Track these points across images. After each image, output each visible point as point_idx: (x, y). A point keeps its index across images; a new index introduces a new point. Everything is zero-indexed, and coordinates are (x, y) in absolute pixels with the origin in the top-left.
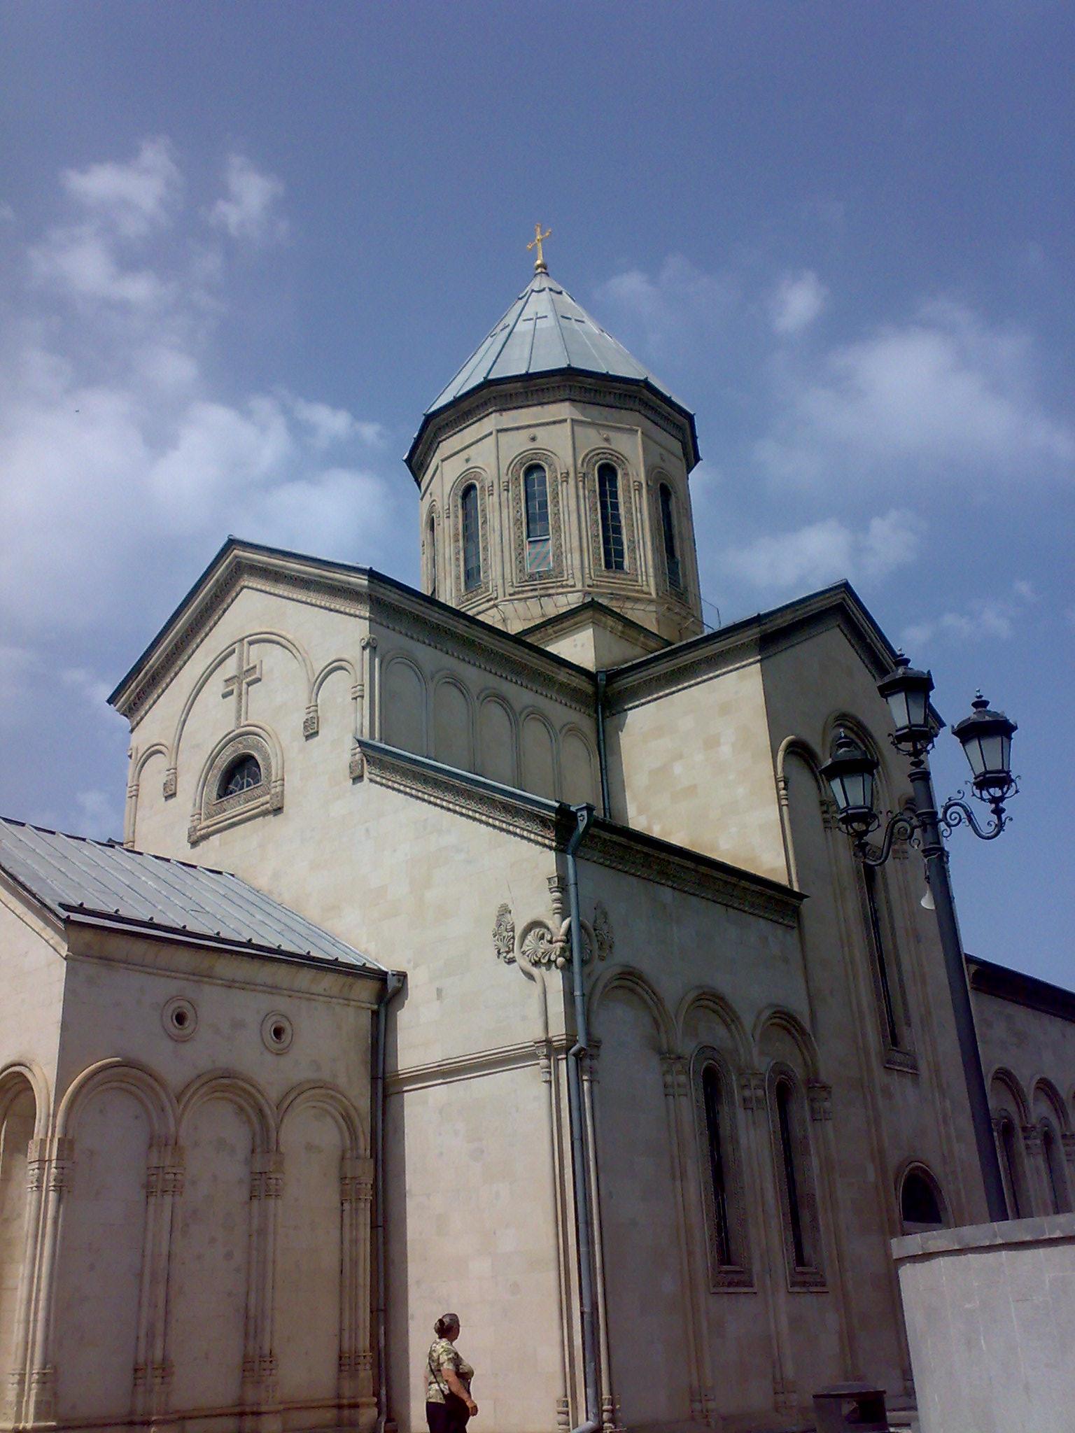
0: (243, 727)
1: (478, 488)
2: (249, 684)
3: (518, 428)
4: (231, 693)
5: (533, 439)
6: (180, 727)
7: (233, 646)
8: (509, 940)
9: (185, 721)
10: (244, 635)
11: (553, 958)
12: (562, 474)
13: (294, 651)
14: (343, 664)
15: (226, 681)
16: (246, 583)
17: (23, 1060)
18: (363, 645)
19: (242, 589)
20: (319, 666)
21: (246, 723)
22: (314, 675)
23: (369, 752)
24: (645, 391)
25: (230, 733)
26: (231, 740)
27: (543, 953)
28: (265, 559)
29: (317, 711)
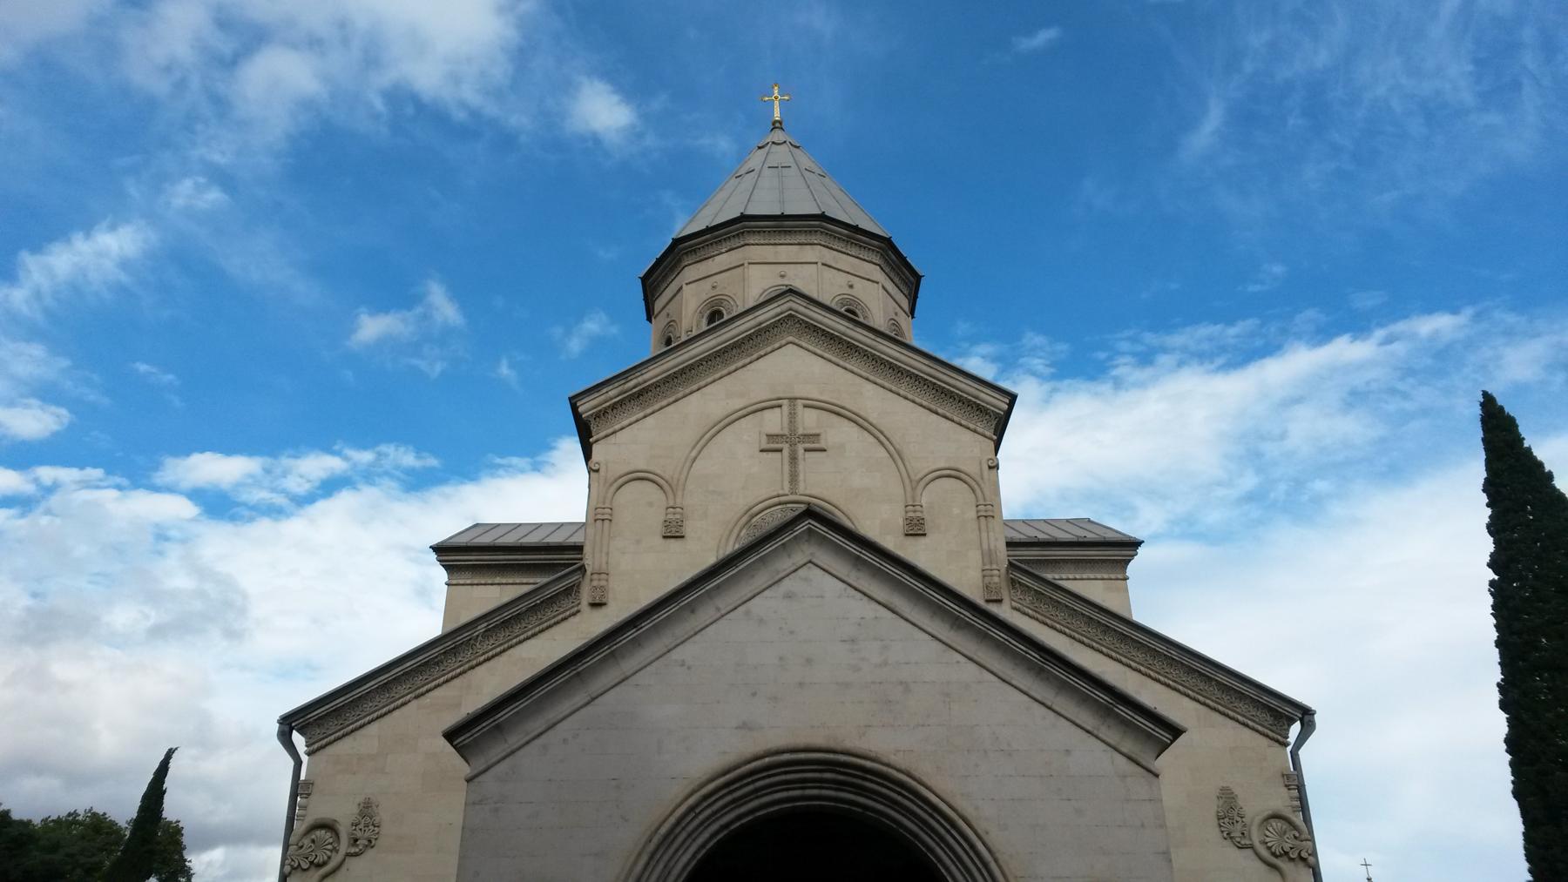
0: (801, 495)
2: (806, 450)
3: (839, 270)
4: (780, 450)
6: (688, 464)
10: (798, 395)
11: (1304, 854)
13: (882, 438)
14: (963, 476)
15: (767, 435)
16: (797, 341)
19: (787, 344)
20: (921, 466)
21: (808, 492)
22: (916, 476)
23: (1026, 580)
25: (778, 496)
26: (780, 504)
27: (1291, 848)
28: (842, 329)
29: (922, 512)
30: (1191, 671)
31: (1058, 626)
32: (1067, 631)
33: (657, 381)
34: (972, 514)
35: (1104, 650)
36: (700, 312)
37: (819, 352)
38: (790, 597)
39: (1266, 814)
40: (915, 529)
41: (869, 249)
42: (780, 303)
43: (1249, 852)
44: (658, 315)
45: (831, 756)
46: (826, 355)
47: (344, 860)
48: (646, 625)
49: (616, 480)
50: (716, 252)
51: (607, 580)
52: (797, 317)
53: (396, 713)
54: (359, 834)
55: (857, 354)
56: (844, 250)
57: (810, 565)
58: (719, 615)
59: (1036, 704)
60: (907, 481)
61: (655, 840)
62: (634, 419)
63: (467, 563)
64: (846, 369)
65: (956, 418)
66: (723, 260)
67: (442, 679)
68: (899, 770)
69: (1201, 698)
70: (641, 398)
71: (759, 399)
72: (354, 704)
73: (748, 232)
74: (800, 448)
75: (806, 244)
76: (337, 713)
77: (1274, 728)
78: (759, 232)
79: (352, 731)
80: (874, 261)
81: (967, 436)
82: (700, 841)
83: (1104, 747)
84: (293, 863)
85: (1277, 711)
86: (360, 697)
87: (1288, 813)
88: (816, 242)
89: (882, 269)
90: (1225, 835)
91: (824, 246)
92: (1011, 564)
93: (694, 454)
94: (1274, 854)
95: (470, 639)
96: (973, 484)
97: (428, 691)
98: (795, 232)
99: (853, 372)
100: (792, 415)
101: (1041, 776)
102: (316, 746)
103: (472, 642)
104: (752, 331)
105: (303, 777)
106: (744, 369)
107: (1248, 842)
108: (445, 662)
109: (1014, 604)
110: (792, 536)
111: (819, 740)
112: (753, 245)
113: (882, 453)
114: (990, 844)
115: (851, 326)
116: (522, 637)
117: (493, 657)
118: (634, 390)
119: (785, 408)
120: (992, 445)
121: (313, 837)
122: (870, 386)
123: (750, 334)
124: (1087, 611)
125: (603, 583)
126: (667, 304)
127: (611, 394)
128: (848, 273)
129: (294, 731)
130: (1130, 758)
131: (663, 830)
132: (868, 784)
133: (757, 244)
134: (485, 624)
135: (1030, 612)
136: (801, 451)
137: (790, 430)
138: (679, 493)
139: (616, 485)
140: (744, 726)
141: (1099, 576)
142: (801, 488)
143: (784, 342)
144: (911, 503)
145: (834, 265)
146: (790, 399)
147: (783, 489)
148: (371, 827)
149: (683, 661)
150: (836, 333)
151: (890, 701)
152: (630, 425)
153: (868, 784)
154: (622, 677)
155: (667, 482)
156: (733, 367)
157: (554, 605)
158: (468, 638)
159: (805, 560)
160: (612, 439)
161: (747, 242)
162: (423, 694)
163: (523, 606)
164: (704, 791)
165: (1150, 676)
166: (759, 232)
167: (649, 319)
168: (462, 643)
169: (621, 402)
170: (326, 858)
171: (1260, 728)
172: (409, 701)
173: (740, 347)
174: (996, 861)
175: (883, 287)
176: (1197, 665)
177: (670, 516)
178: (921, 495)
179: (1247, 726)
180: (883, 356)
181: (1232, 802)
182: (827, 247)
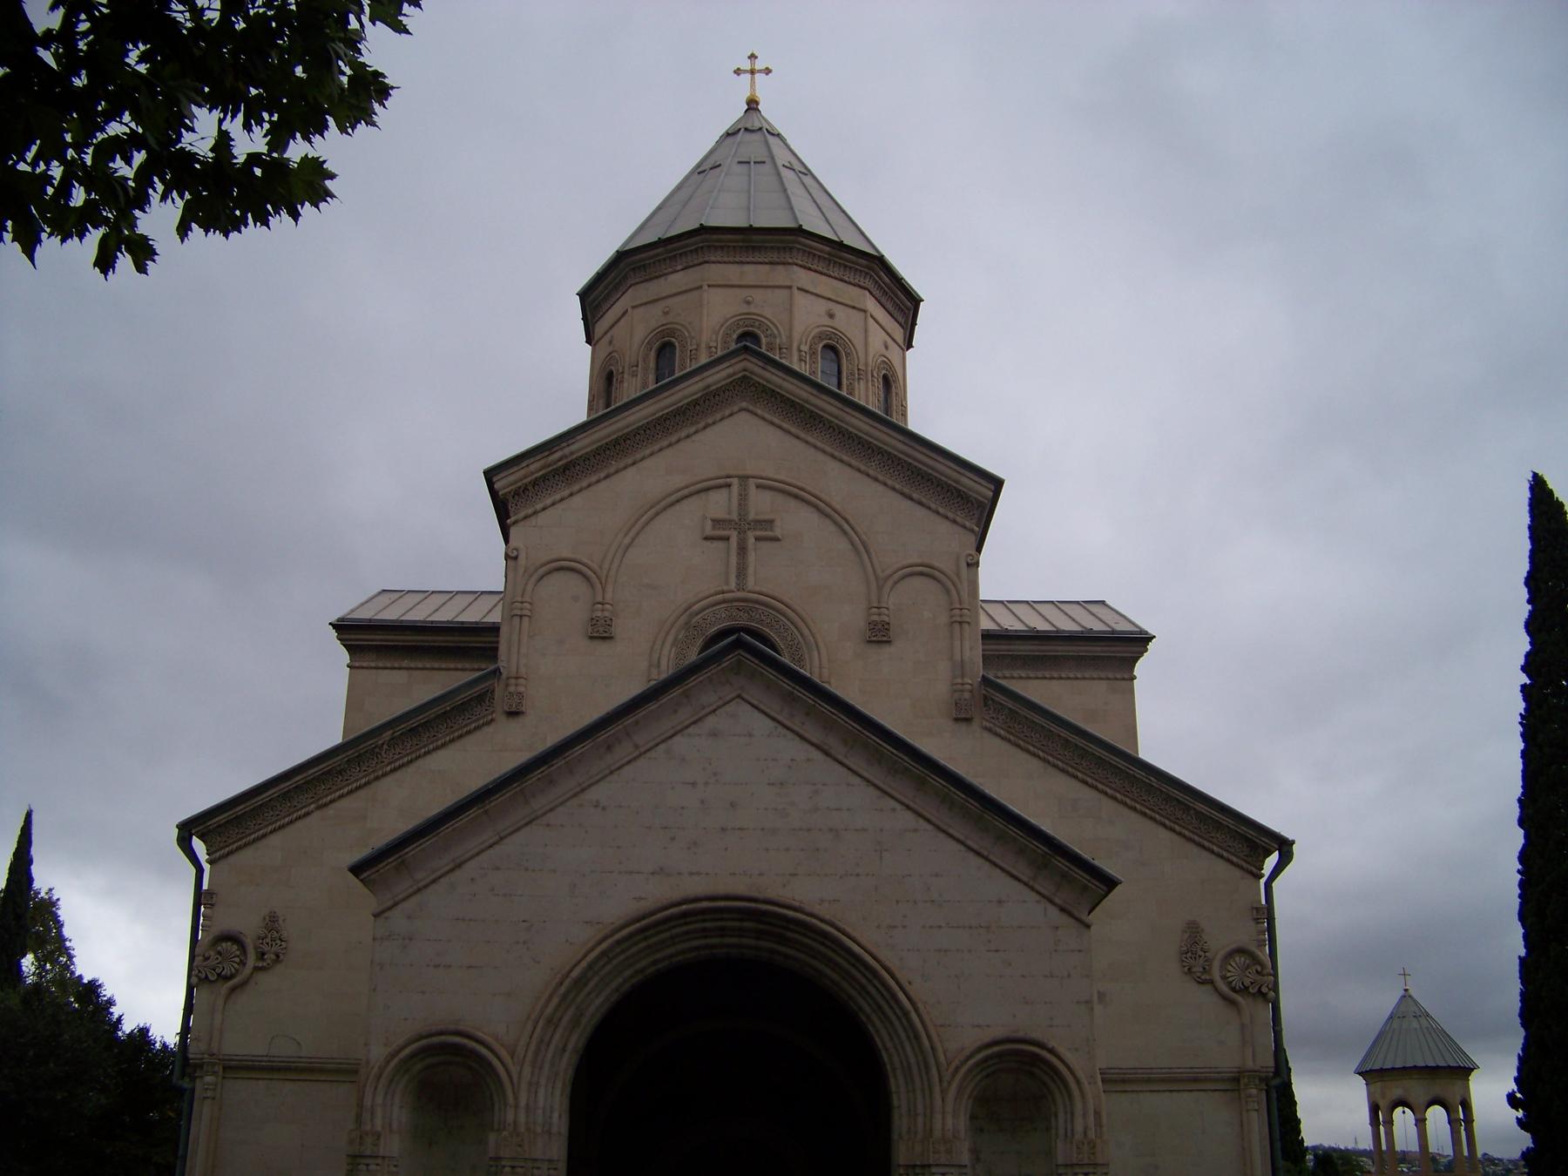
0: (749, 592)
1: (764, 340)
2: (757, 539)
4: (727, 539)
5: (831, 316)
7: (728, 480)
8: (1206, 961)
9: (628, 547)
10: (749, 472)
11: (1264, 990)
12: (859, 369)
13: (846, 526)
14: (937, 574)
15: (713, 520)
16: (751, 408)
17: (1021, 1034)
18: (970, 562)
19: (740, 410)
21: (757, 589)
22: (883, 571)
23: (999, 697)
24: (912, 312)
25: (723, 593)
26: (724, 601)
27: (1252, 983)
28: (804, 395)
30: (1169, 799)
31: (1031, 748)
32: (1041, 754)
33: (587, 453)
34: (943, 619)
35: (1080, 775)
36: (648, 343)
37: (776, 421)
38: (715, 735)
39: (1228, 949)
40: (879, 634)
41: (856, 270)
42: (733, 361)
43: (1209, 987)
44: (597, 342)
45: (753, 905)
46: (785, 425)
47: (252, 973)
48: (559, 762)
49: (536, 570)
50: (670, 270)
51: (526, 687)
52: (752, 379)
53: (299, 824)
54: (266, 948)
55: (821, 425)
56: (825, 271)
57: (737, 700)
58: (637, 753)
59: (971, 855)
60: (872, 578)
61: (567, 982)
62: (558, 497)
63: (370, 643)
64: (807, 442)
65: (933, 506)
66: (678, 280)
67: (346, 790)
68: (822, 920)
69: (1177, 828)
70: (567, 472)
71: (704, 477)
72: (255, 812)
73: (709, 247)
74: (751, 536)
75: (778, 263)
76: (237, 821)
77: (1249, 860)
78: (722, 248)
79: (254, 841)
80: (862, 284)
81: (944, 527)
82: (614, 985)
83: (1038, 897)
84: (200, 974)
85: (1255, 842)
86: (261, 805)
87: (1253, 948)
88: (790, 261)
89: (871, 293)
90: (1186, 969)
91: (801, 266)
92: (983, 676)
93: (627, 541)
94: (1234, 990)
95: (375, 747)
96: (949, 584)
97: (332, 802)
98: (766, 248)
99: (815, 447)
100: (743, 497)
101: (971, 927)
102: (218, 854)
103: (377, 750)
104: (699, 395)
105: (205, 887)
106: (689, 440)
107: (1208, 978)
108: (348, 772)
109: (988, 725)
110: (719, 668)
111: (740, 888)
112: (714, 262)
113: (843, 545)
114: (911, 994)
115: (815, 392)
116: (431, 747)
117: (400, 767)
118: (560, 463)
119: (735, 489)
120: (972, 540)
121: (219, 948)
122: (837, 465)
123: (697, 399)
124: (1064, 733)
125: (521, 689)
126: (613, 326)
127: (532, 468)
128: (829, 299)
129: (194, 837)
130: (1062, 910)
131: (575, 974)
132: (789, 934)
133: (720, 263)
134: (391, 732)
135: (1002, 732)
136: (751, 540)
137: (740, 515)
138: (609, 589)
139: (536, 576)
140: (660, 872)
141: (1103, 675)
142: (750, 582)
143: (736, 408)
144: (875, 605)
145: (812, 290)
146: (739, 477)
147: (727, 583)
148: (279, 942)
149: (598, 801)
150: (798, 401)
151: (818, 850)
152: (553, 504)
153: (789, 934)
154: (533, 816)
155: (595, 573)
156: (674, 438)
157: (466, 713)
158: (373, 746)
159: (734, 695)
160: (533, 520)
161: (706, 259)
162: (325, 805)
163: (432, 713)
164: (617, 937)
165: (1125, 804)
166: (722, 248)
167: (589, 341)
168: (366, 752)
169: (544, 478)
170: (233, 969)
171: (1235, 859)
172: (312, 812)
173: (684, 413)
174: (916, 1010)
175: (872, 316)
176: (1176, 793)
177: (599, 614)
178: (889, 596)
179: (1222, 857)
180: (851, 429)
181: (1196, 937)
182: (805, 268)
